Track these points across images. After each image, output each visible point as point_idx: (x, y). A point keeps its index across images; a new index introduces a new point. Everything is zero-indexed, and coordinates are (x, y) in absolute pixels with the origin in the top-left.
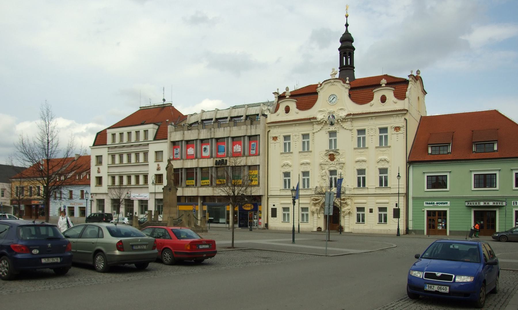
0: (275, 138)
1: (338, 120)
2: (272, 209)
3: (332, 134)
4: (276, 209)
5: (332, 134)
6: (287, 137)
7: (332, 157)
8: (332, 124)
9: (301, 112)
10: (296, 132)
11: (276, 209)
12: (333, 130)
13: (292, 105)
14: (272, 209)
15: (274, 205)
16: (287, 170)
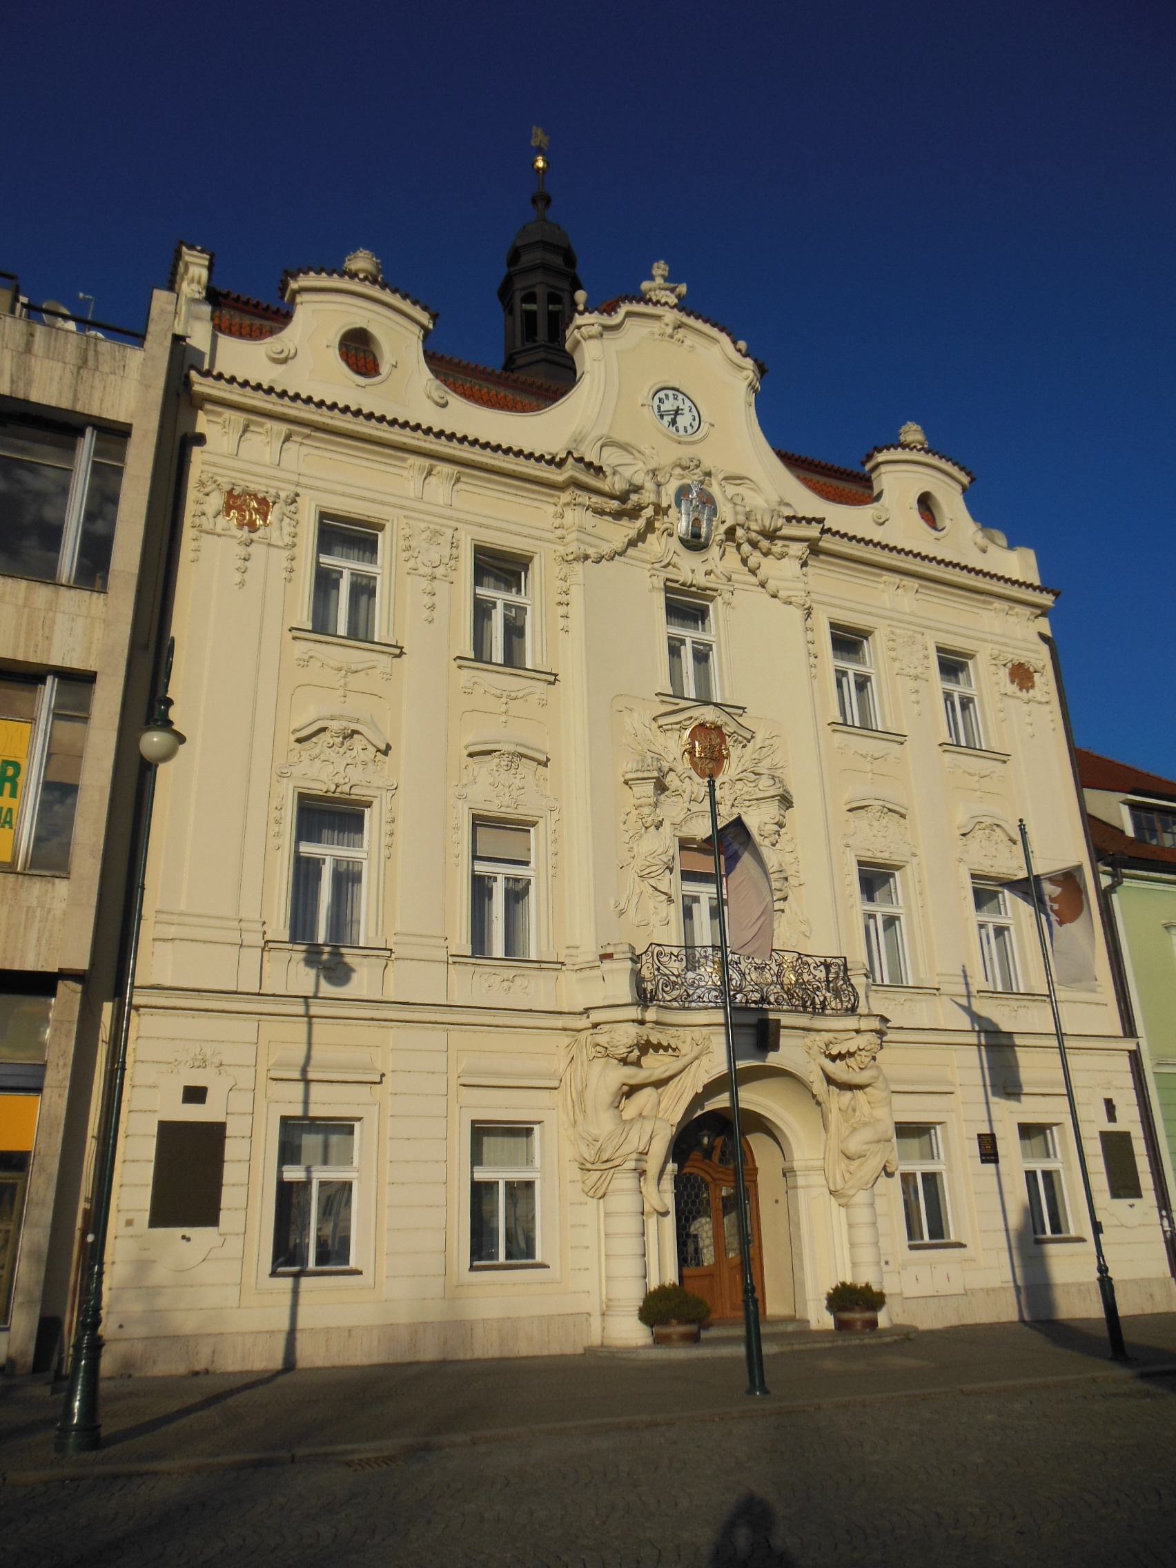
0: (247, 506)
1: (730, 532)
2: (169, 1133)
3: (686, 607)
4: (215, 1134)
5: (686, 607)
6: (346, 535)
7: (710, 749)
8: (695, 543)
9: (456, 401)
10: (429, 522)
11: (215, 1134)
12: (701, 580)
13: (400, 336)
14: (169, 1133)
15: (195, 1095)
16: (326, 774)
